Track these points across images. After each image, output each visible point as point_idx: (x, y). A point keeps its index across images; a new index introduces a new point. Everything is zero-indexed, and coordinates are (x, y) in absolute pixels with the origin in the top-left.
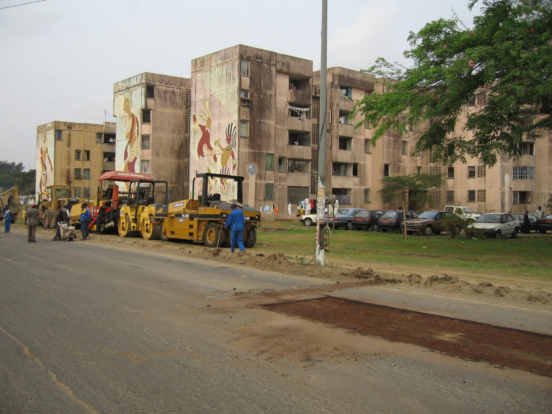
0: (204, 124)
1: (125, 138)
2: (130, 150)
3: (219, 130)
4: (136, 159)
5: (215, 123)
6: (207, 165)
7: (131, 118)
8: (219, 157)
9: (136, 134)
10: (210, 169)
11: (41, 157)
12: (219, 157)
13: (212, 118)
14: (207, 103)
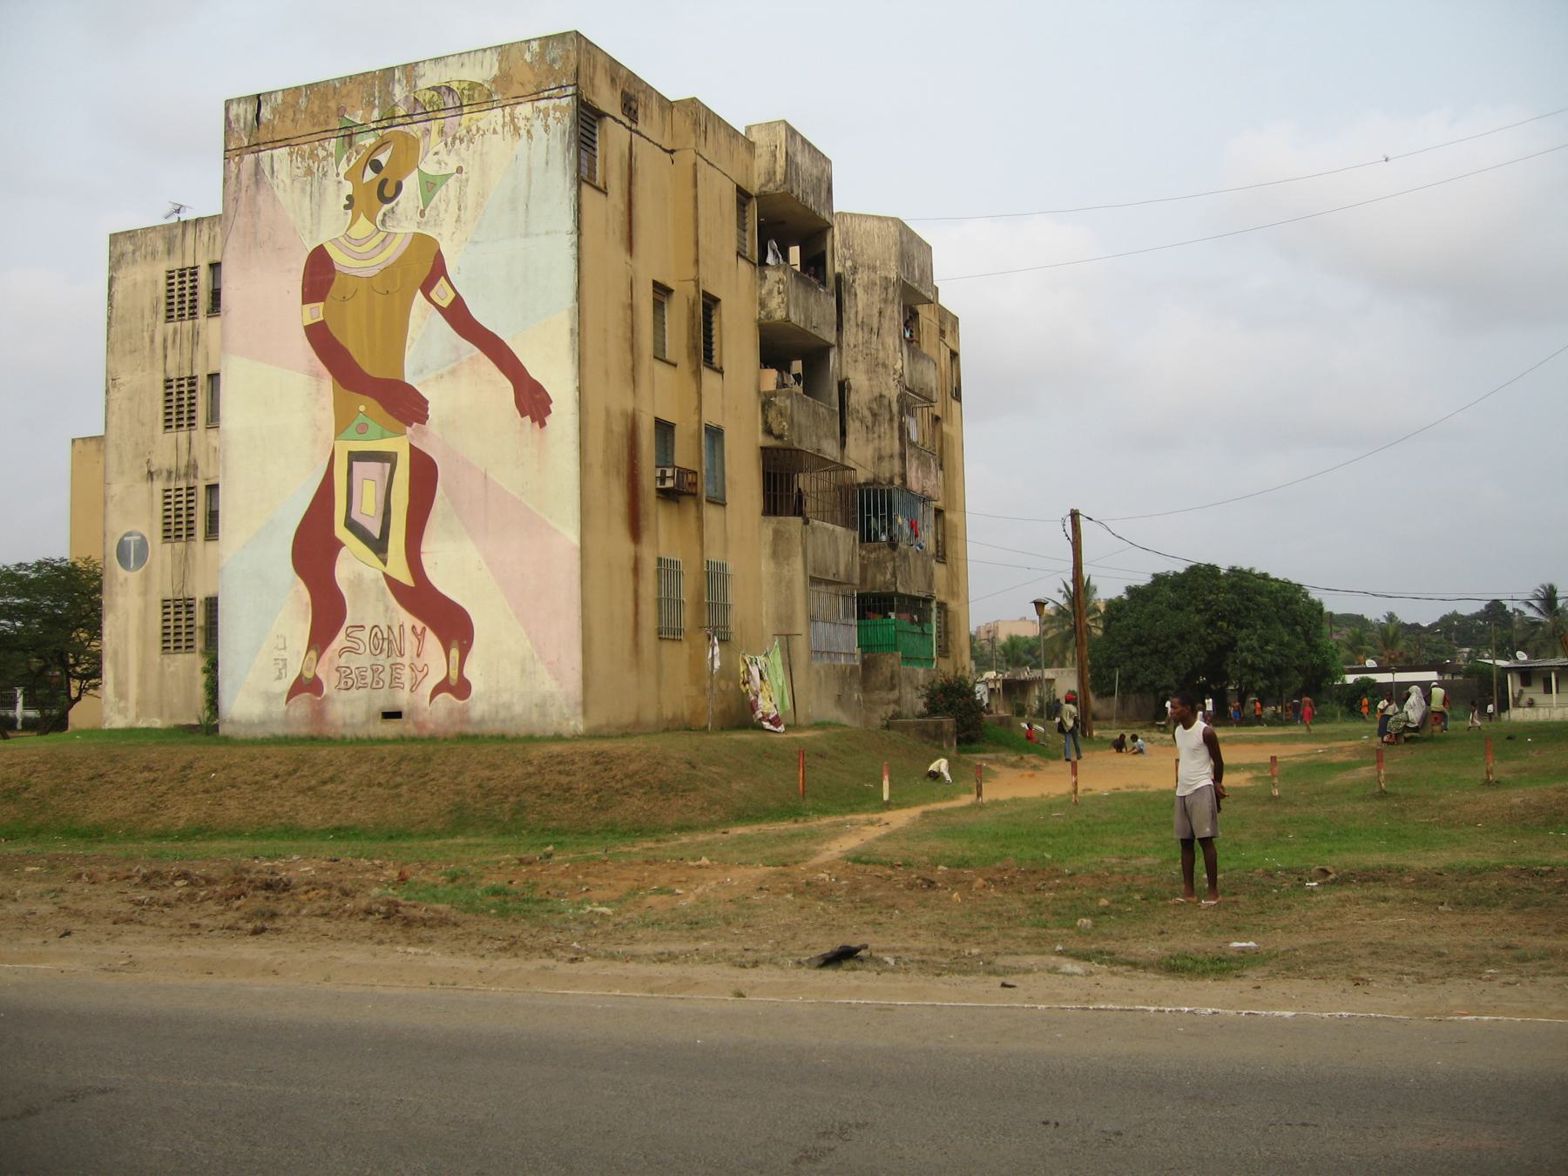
11: (319, 336)
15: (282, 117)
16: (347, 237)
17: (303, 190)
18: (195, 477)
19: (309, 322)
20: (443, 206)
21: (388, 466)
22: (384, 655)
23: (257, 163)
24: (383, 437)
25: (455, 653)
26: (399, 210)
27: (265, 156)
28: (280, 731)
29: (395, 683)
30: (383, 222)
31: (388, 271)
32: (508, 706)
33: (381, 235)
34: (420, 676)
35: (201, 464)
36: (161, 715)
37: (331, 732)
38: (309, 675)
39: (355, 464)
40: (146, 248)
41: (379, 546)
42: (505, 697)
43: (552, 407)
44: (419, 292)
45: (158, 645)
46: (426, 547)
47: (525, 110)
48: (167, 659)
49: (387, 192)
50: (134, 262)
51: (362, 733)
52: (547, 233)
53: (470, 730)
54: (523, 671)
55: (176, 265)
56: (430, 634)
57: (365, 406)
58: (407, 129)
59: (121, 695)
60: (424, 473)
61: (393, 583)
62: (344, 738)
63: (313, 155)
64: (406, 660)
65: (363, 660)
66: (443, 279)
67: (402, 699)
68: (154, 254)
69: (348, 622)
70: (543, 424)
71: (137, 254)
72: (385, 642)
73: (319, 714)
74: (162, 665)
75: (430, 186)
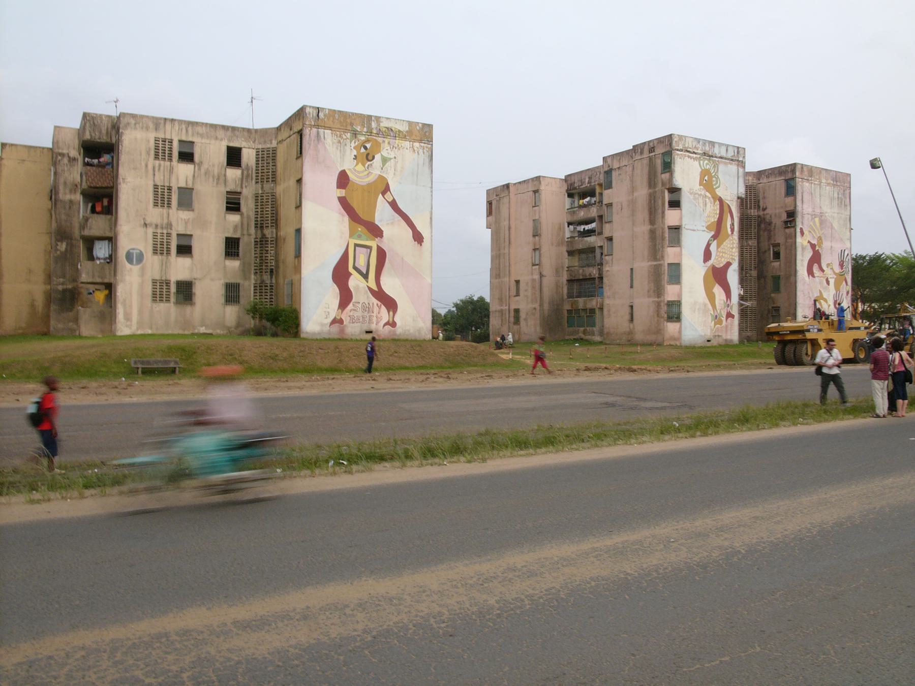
0: (814, 242)
2: (718, 248)
3: (832, 253)
4: (728, 264)
5: (826, 244)
6: (819, 287)
7: (717, 202)
8: (832, 281)
9: (729, 230)
10: (823, 292)
11: (343, 201)
12: (832, 281)
13: (823, 238)
14: (817, 220)
15: (328, 119)
16: (354, 169)
17: (337, 148)
18: (171, 229)
19: (339, 195)
20: (389, 168)
21: (369, 250)
22: (366, 312)
23: (318, 133)
24: (367, 240)
25: (391, 313)
26: (374, 165)
27: (321, 131)
28: (327, 337)
29: (370, 321)
30: (368, 168)
31: (369, 185)
32: (409, 331)
33: (366, 173)
34: (379, 320)
35: (174, 224)
36: (151, 328)
37: (345, 337)
38: (338, 318)
39: (357, 248)
40: (142, 124)
41: (366, 276)
42: (408, 328)
43: (424, 240)
44: (381, 195)
45: (150, 298)
46: (382, 278)
47: (417, 145)
48: (155, 305)
49: (369, 157)
50: (135, 128)
51: (358, 338)
52: (423, 186)
53: (397, 338)
54: (414, 320)
55: (161, 135)
56: (383, 306)
57: (360, 229)
58: (377, 138)
59: (128, 318)
60: (382, 255)
61: (370, 289)
62: (352, 339)
63: (340, 136)
64: (375, 314)
65: (359, 314)
66: (389, 192)
67: (373, 327)
68: (147, 128)
69: (354, 300)
70: (421, 245)
71: (137, 125)
72: (367, 308)
73: (342, 331)
74: (152, 307)
75: (385, 160)
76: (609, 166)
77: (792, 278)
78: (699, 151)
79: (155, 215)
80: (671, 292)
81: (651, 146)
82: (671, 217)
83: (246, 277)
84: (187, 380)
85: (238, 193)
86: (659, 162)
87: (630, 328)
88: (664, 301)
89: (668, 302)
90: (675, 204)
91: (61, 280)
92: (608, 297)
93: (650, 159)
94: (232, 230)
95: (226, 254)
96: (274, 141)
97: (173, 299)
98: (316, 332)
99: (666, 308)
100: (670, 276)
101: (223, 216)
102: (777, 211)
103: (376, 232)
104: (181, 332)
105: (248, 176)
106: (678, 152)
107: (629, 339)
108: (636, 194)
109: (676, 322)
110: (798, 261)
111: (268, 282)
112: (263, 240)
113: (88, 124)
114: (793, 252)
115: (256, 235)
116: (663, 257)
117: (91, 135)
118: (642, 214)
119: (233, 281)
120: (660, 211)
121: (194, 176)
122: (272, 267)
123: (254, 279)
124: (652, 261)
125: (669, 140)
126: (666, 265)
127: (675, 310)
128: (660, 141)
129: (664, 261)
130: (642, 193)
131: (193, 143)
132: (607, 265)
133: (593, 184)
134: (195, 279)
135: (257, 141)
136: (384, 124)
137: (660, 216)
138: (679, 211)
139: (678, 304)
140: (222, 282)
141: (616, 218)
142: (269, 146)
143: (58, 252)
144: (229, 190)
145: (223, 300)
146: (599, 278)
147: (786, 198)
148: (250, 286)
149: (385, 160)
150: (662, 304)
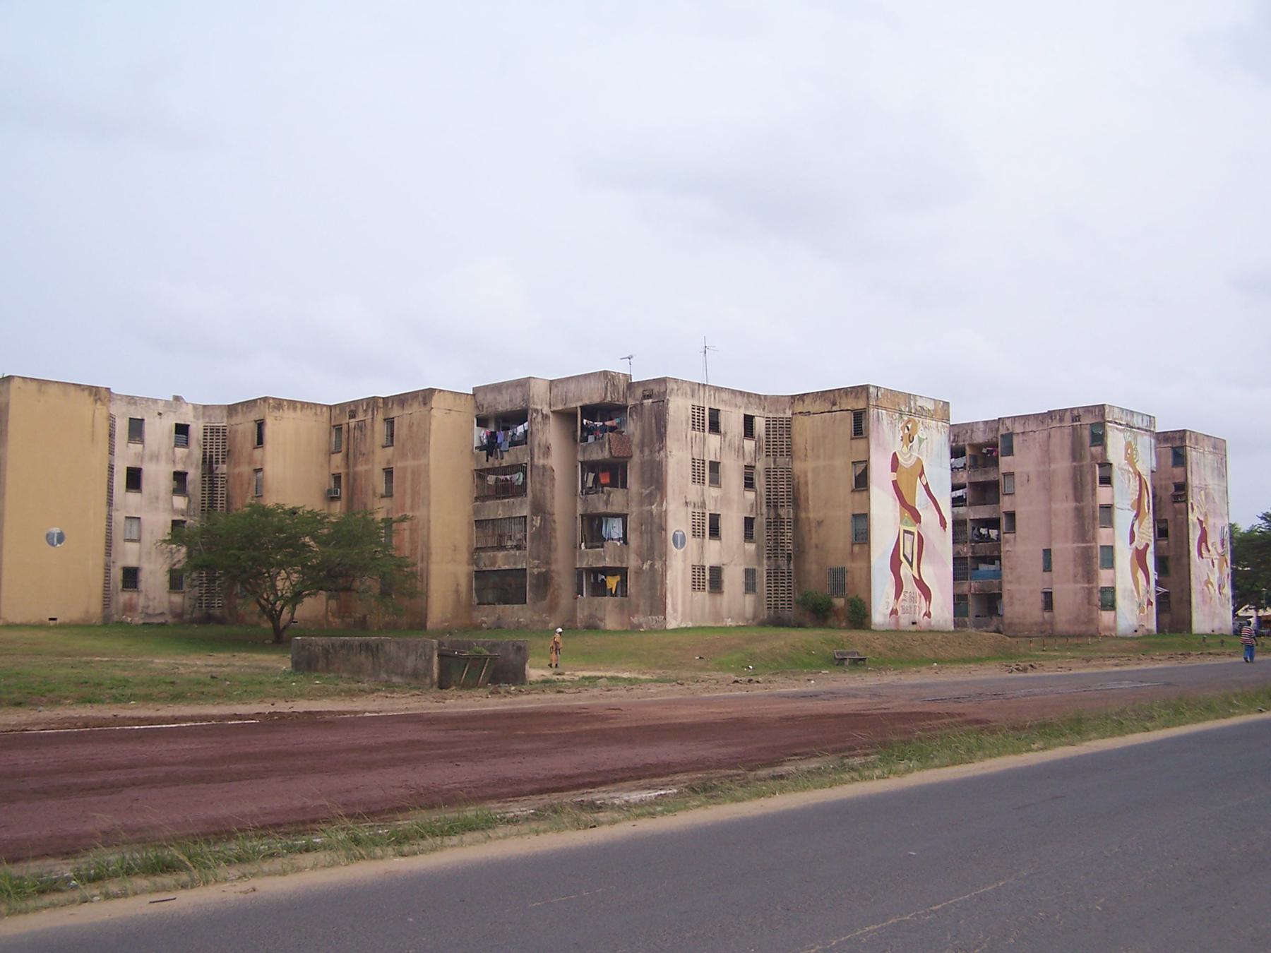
1: (1130, 508)
4: (1147, 546)
7: (1138, 478)
9: (1146, 508)
11: (895, 483)
24: (911, 526)
25: (928, 603)
32: (939, 621)
36: (691, 620)
37: (900, 629)
47: (940, 424)
53: (932, 629)
59: (675, 610)
69: (904, 590)
75: (921, 441)
76: (1008, 429)
77: (1185, 561)
78: (1124, 423)
79: (693, 491)
80: (1104, 578)
81: (1076, 415)
82: (1103, 495)
83: (760, 563)
84: (466, 692)
85: (751, 466)
86: (1086, 434)
87: (1044, 618)
88: (1097, 587)
89: (1102, 588)
90: (1106, 481)
91: (536, 561)
92: (1010, 582)
93: (1074, 428)
94: (749, 509)
95: (745, 537)
96: (787, 411)
97: (707, 588)
98: (881, 623)
99: (1099, 594)
100: (1102, 560)
101: (742, 493)
102: (1163, 483)
103: (916, 518)
104: (713, 625)
105: (760, 447)
106: (1109, 424)
107: (1043, 630)
108: (1053, 466)
109: (1111, 610)
110: (1190, 540)
111: (785, 568)
112: (779, 520)
113: (609, 384)
114: (1185, 530)
115: (768, 515)
116: (1094, 539)
117: (611, 397)
118: (1063, 489)
119: (750, 567)
120: (1089, 487)
121: (721, 448)
122: (789, 552)
123: (767, 564)
124: (1079, 542)
125: (1099, 411)
126: (1099, 547)
127: (1109, 596)
128: (1088, 410)
129: (1096, 542)
130: (1062, 465)
131: (719, 410)
132: (1007, 545)
133: (961, 443)
134: (723, 565)
135: (766, 409)
136: (920, 403)
137: (1090, 492)
138: (1111, 488)
139: (1112, 590)
140: (743, 567)
141: (1019, 490)
142: (782, 415)
143: (534, 528)
144: (746, 464)
145: (743, 589)
146: (971, 557)
147: (1174, 469)
148: (763, 572)
149: (921, 441)
150: (1095, 591)
